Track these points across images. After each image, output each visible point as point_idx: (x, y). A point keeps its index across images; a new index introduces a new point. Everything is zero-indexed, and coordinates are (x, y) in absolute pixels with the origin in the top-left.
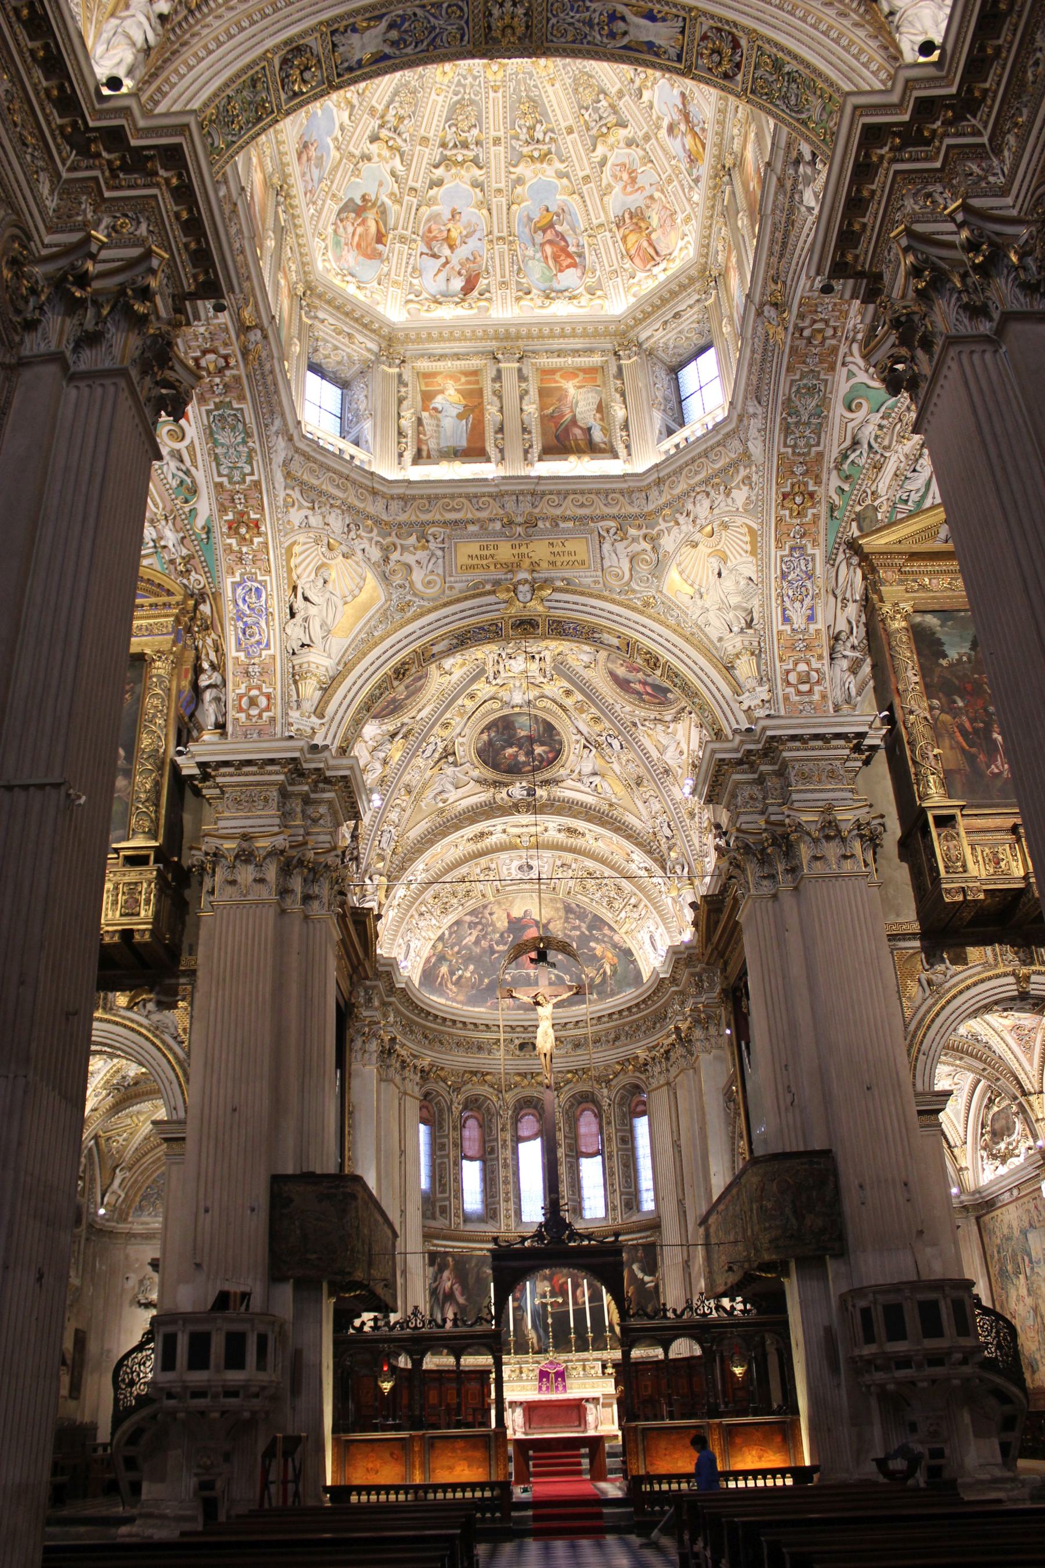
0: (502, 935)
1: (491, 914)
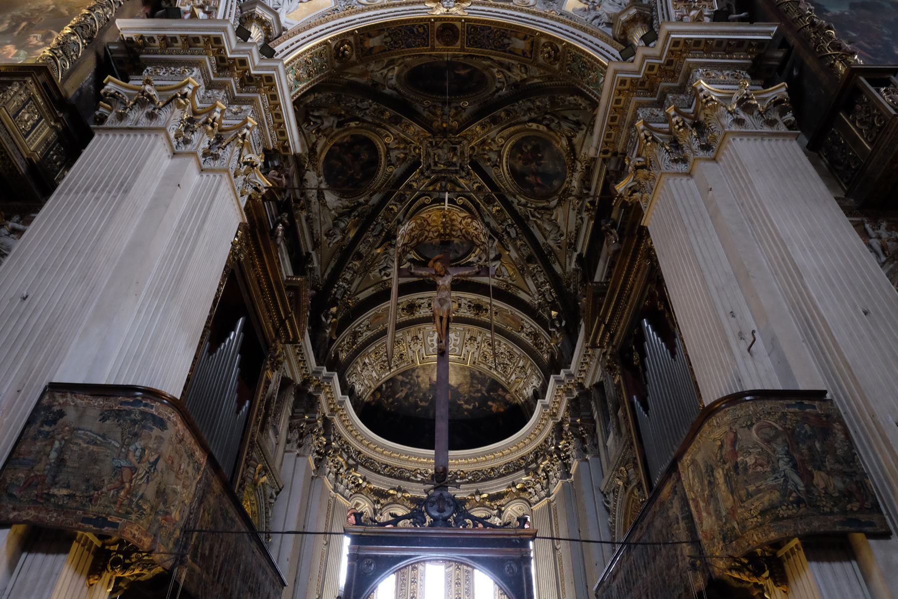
0: (424, 394)
1: (418, 377)
